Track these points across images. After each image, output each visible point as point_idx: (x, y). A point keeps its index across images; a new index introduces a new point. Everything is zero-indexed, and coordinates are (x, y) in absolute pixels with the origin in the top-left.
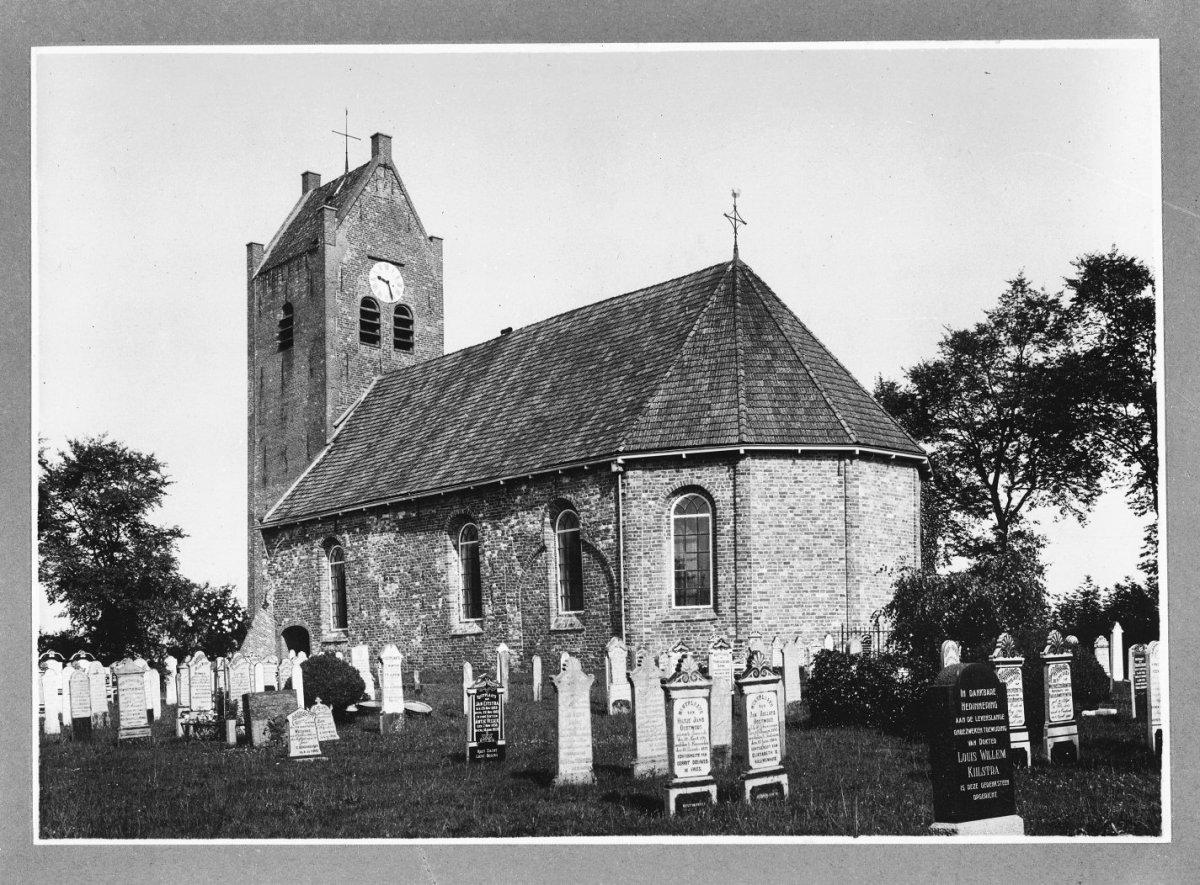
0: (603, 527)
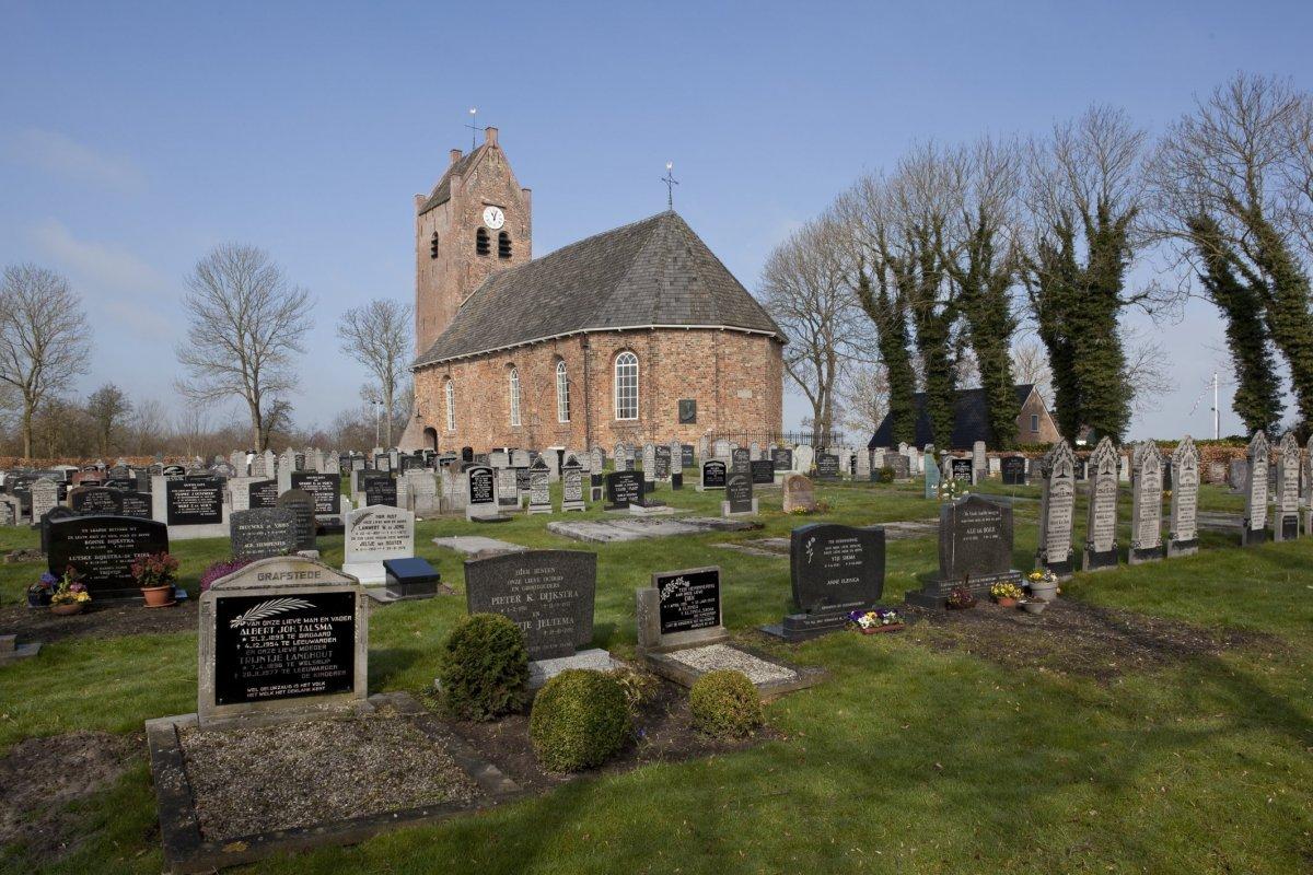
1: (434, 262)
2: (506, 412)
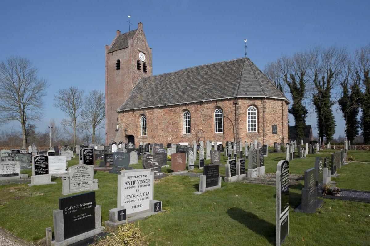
0: (230, 113)
1: (118, 71)
2: (181, 129)
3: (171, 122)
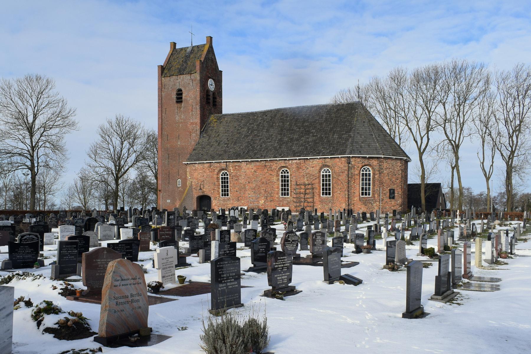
1: (179, 105)
3: (264, 180)
